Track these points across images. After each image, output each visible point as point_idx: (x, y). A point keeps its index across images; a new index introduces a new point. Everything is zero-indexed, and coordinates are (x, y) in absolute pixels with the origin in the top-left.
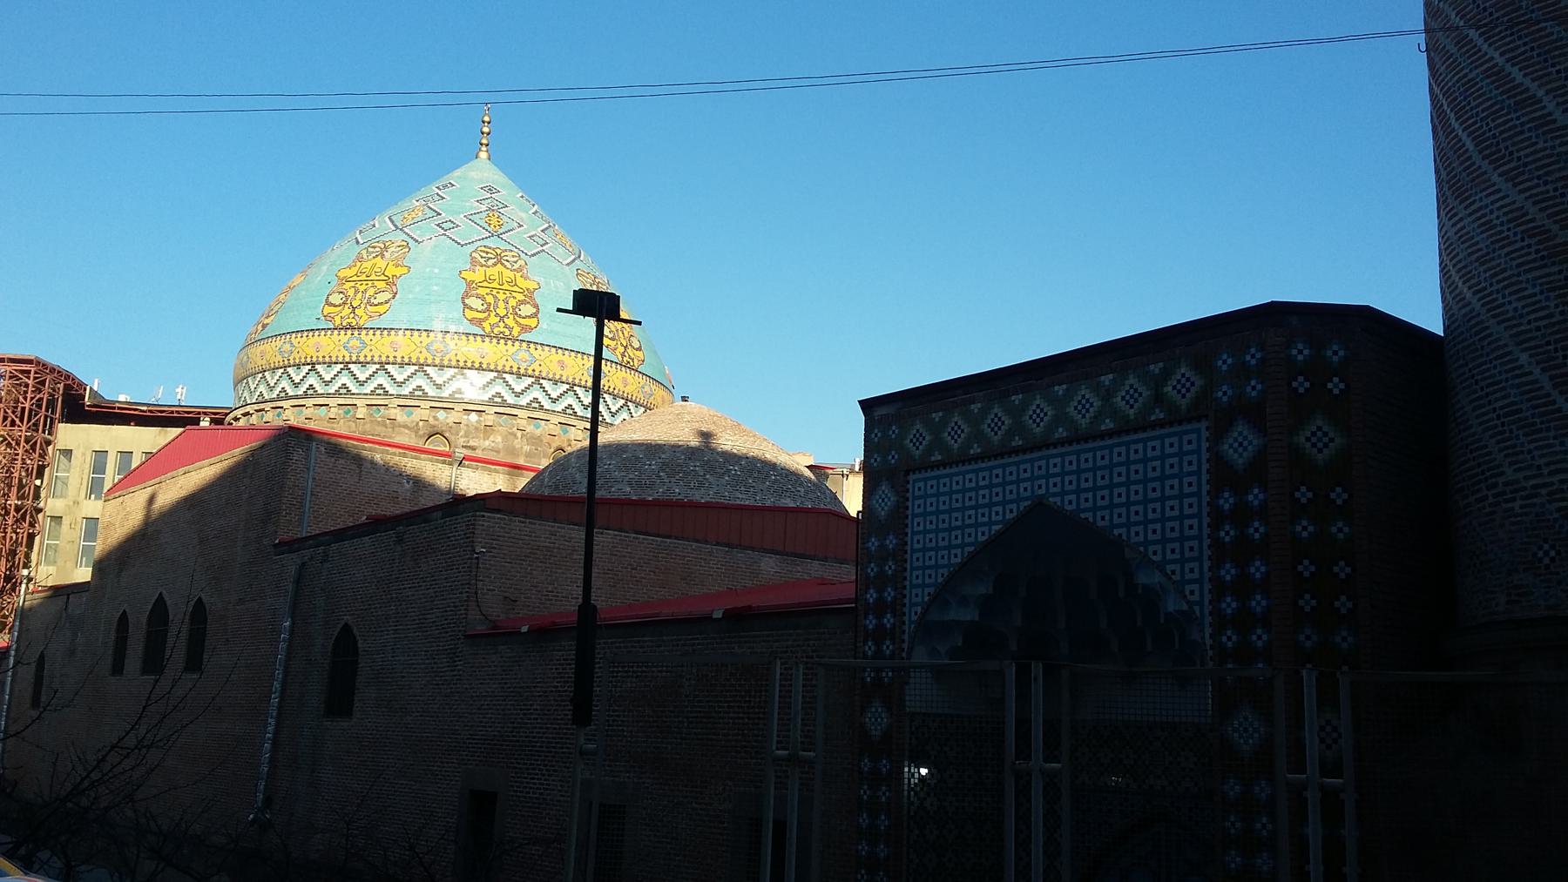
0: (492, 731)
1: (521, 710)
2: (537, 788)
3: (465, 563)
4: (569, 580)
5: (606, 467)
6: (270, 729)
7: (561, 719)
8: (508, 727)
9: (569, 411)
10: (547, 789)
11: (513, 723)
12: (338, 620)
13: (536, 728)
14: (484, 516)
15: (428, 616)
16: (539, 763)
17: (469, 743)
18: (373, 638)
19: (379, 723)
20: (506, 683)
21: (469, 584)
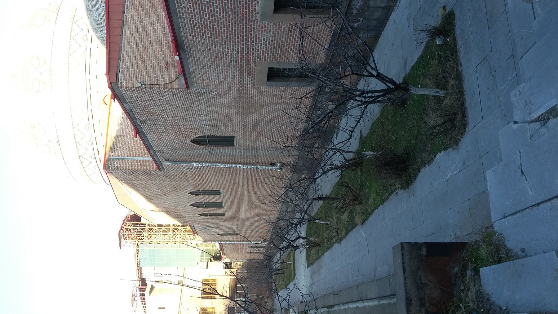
0: (236, 72)
1: (224, 57)
2: (266, 46)
3: (149, 91)
4: (154, 33)
5: (98, 16)
6: (241, 166)
7: (227, 34)
8: (234, 64)
9: (85, 38)
10: (267, 40)
11: (231, 61)
12: (189, 145)
13: (233, 49)
14: (121, 82)
15: (181, 107)
16: (252, 45)
17: (243, 83)
18: (196, 130)
19: (236, 125)
20: (210, 66)
21: (159, 88)
